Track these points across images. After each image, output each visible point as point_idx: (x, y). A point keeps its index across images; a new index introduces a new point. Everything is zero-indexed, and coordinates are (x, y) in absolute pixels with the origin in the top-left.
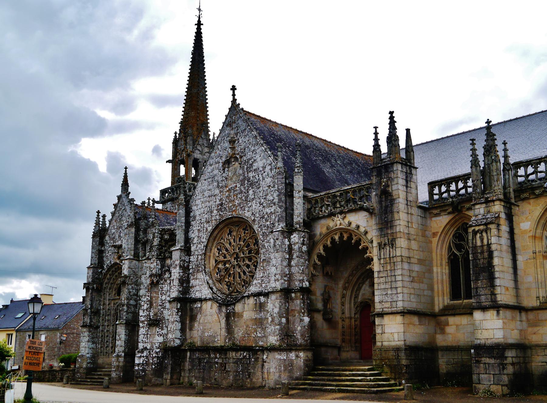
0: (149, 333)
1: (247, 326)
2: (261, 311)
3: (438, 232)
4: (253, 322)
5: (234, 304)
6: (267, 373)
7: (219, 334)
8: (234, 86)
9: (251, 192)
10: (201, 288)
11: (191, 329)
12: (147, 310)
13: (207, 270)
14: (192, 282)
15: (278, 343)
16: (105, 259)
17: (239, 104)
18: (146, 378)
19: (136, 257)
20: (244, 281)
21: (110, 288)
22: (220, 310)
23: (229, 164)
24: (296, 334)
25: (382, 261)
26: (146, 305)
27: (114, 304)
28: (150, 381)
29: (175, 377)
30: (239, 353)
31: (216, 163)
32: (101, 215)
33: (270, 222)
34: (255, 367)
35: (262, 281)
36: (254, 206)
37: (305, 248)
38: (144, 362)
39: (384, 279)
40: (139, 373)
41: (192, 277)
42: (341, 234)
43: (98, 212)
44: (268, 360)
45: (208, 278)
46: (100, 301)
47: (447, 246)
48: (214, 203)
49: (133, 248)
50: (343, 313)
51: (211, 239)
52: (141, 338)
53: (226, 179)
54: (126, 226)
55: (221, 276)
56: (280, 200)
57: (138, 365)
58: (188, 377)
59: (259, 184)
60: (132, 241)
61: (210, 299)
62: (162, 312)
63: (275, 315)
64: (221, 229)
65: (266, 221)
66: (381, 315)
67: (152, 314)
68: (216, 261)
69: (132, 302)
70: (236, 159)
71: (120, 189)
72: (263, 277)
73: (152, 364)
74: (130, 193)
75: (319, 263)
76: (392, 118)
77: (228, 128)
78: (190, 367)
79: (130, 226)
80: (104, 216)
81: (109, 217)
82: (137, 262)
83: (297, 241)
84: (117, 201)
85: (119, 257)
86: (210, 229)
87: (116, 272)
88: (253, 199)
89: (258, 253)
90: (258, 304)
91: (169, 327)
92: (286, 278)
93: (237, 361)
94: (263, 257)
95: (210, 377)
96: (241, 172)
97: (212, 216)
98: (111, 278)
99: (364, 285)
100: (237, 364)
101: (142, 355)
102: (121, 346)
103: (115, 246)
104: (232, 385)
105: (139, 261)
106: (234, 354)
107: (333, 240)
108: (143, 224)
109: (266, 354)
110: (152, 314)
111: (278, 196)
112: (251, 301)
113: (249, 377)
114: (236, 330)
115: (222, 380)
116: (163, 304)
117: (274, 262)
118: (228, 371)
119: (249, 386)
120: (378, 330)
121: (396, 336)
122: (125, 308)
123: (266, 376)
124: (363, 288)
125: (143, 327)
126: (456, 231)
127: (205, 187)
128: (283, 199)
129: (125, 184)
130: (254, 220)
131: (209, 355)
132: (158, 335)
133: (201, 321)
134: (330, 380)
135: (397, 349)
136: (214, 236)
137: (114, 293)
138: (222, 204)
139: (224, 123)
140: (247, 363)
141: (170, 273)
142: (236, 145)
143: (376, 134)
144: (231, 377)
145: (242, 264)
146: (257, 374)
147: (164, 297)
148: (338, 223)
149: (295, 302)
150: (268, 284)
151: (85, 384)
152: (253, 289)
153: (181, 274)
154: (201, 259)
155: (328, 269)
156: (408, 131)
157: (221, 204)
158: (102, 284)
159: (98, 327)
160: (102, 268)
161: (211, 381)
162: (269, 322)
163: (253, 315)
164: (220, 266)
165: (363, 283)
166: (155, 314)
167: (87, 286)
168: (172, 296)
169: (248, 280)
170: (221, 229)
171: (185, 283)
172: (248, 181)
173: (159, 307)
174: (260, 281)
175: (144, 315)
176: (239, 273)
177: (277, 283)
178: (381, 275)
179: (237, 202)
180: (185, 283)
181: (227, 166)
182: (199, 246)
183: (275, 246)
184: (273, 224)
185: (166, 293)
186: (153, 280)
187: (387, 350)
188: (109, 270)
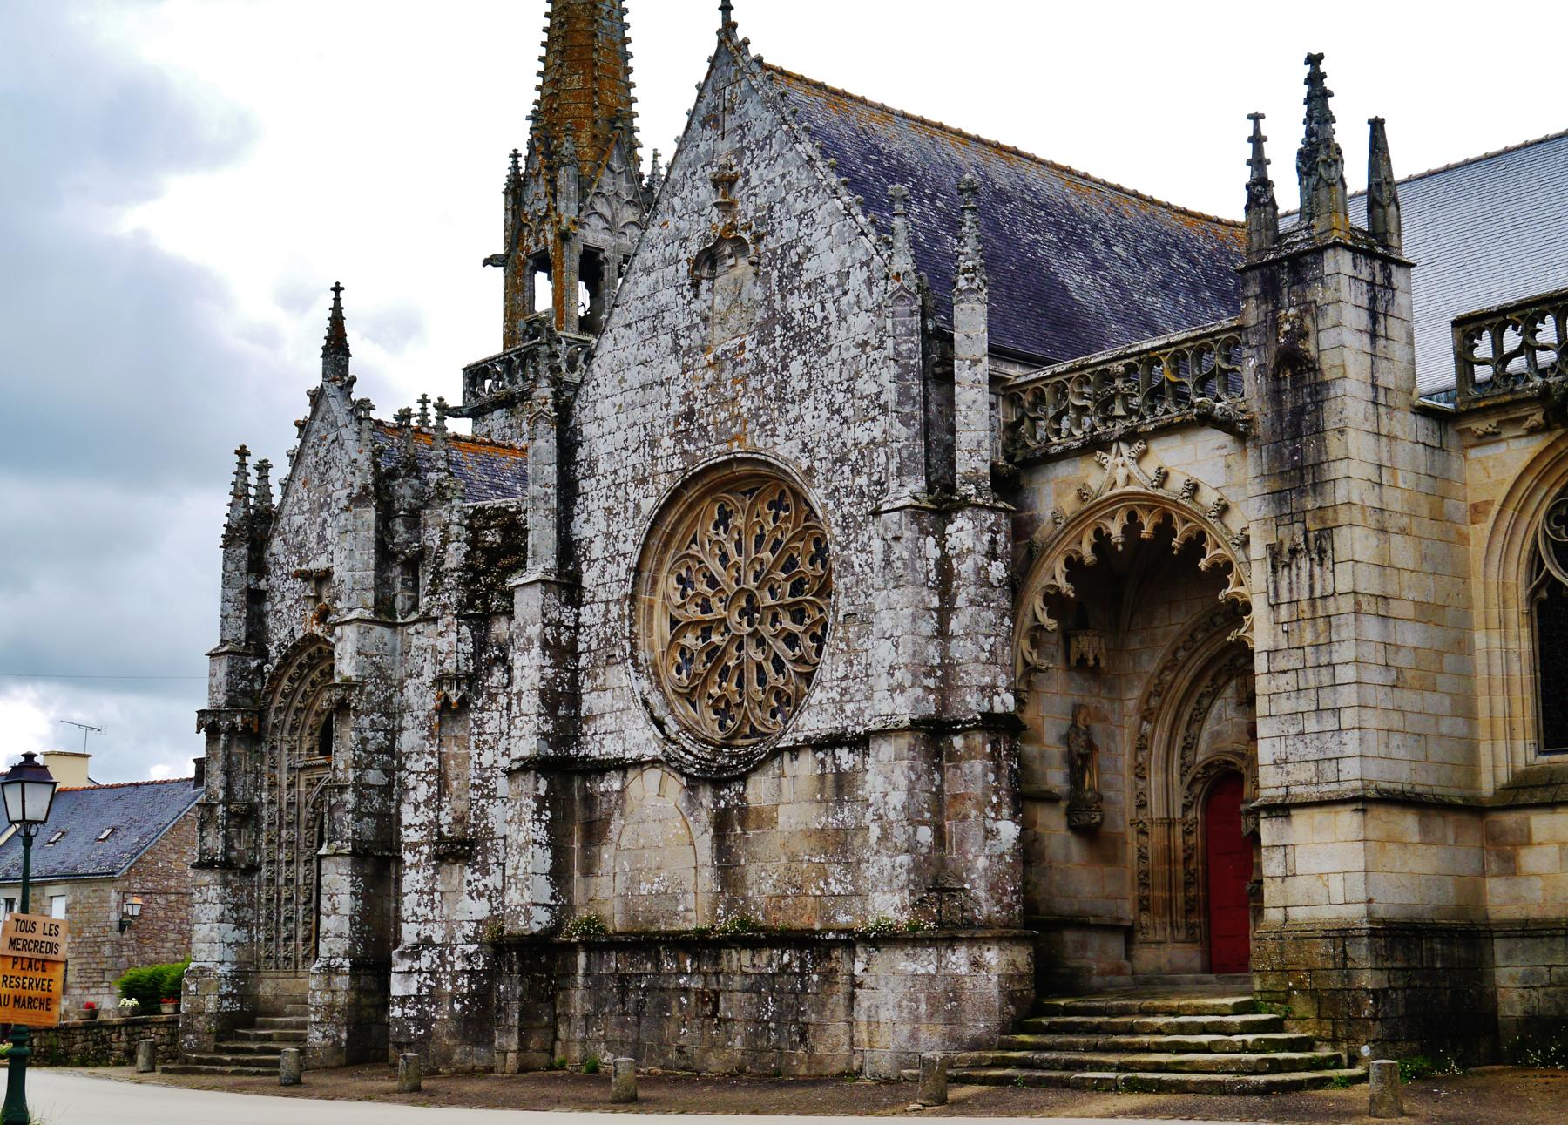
0: (439, 887)
1: (793, 858)
2: (840, 803)
3: (1489, 503)
4: (813, 842)
5: (743, 778)
6: (869, 1023)
7: (688, 886)
9: (796, 368)
10: (619, 721)
11: (588, 872)
12: (427, 802)
13: (641, 657)
14: (590, 701)
15: (904, 918)
16: (270, 622)
17: (746, 43)
18: (432, 1049)
19: (384, 613)
20: (779, 694)
21: (293, 729)
22: (692, 800)
23: (713, 267)
24: (972, 882)
25: (1284, 610)
27: (310, 784)
28: (446, 1059)
29: (534, 1043)
30: (766, 954)
31: (666, 263)
32: (252, 462)
33: (870, 475)
34: (824, 1005)
35: (844, 691)
36: (808, 418)
37: (998, 571)
38: (424, 991)
39: (1291, 677)
40: (404, 1031)
41: (587, 684)
42: (1132, 516)
43: (242, 452)
44: (869, 980)
45: (645, 684)
46: (259, 774)
47: (1525, 554)
48: (662, 411)
49: (371, 582)
50: (1142, 806)
51: (654, 541)
52: (409, 904)
53: (705, 319)
54: (344, 502)
55: (693, 676)
56: (904, 395)
57: (403, 1000)
58: (583, 1042)
59: (827, 337)
60: (367, 556)
61: (655, 762)
62: (483, 810)
63: (892, 816)
64: (691, 507)
65: (856, 471)
66: (1282, 809)
67: (445, 819)
68: (674, 622)
69: (374, 777)
70: (740, 246)
71: (317, 365)
72: (846, 677)
73: (453, 998)
74: (354, 379)
75: (1051, 624)
76: (1315, 80)
77: (708, 133)
78: (588, 1007)
79: (357, 500)
80: (263, 467)
81: (280, 470)
82: (387, 632)
83: (969, 543)
84: (308, 411)
85: (323, 616)
86: (648, 505)
87: (312, 668)
88: (805, 393)
89: (825, 589)
90: (830, 778)
91: (508, 863)
92: (931, 682)
93: (759, 985)
94: (844, 606)
95: (661, 1043)
96: (759, 293)
97: (654, 458)
98: (294, 692)
99: (1218, 703)
100: (759, 993)
101: (416, 966)
102: (340, 935)
103: (306, 576)
104: (742, 1070)
105: (393, 626)
106: (746, 956)
107: (1102, 538)
108: (405, 491)
109: (864, 957)
110: (445, 819)
111: (898, 378)
112: (807, 764)
113: (803, 1039)
114: (752, 872)
115: (706, 1051)
116: (487, 780)
117: (885, 622)
118: (726, 1020)
119: (802, 1071)
120: (1271, 865)
121: (1336, 884)
122: (349, 797)
123: (865, 1036)
124: (1214, 712)
125: (415, 865)
126: (1559, 495)
127: (629, 354)
128: (916, 389)
129: (336, 347)
130: (810, 471)
131: (658, 963)
132: (470, 893)
133: (624, 842)
134: (1096, 1049)
135: (1342, 934)
136: (664, 529)
137: (306, 745)
138: (691, 409)
139: (692, 114)
140: (793, 991)
141: (509, 670)
142: (738, 192)
143: (1257, 140)
144: (738, 1043)
145: (767, 631)
146: (832, 1030)
147: (487, 758)
148: (1120, 474)
149: (966, 766)
150: (863, 704)
151: (214, 1072)
152: (812, 722)
153: (549, 672)
154: (621, 618)
155: (1087, 645)
156: (1377, 125)
157: (689, 415)
158: (262, 714)
159: (253, 869)
160: (263, 654)
161: (664, 1055)
162: (873, 840)
164: (691, 640)
165: (1215, 694)
166: (460, 820)
167: (209, 723)
168: (516, 754)
169: (791, 689)
170: (691, 507)
171: (563, 703)
172: (785, 327)
173: (473, 794)
174: (835, 694)
175: (417, 821)
176: (760, 666)
177: (900, 699)
178: (1281, 663)
179: (745, 405)
180: (563, 703)
181: (705, 272)
182: (612, 568)
183: (888, 563)
184: (879, 483)
185: (497, 741)
186: (447, 697)
187: (1304, 937)
188: (286, 661)
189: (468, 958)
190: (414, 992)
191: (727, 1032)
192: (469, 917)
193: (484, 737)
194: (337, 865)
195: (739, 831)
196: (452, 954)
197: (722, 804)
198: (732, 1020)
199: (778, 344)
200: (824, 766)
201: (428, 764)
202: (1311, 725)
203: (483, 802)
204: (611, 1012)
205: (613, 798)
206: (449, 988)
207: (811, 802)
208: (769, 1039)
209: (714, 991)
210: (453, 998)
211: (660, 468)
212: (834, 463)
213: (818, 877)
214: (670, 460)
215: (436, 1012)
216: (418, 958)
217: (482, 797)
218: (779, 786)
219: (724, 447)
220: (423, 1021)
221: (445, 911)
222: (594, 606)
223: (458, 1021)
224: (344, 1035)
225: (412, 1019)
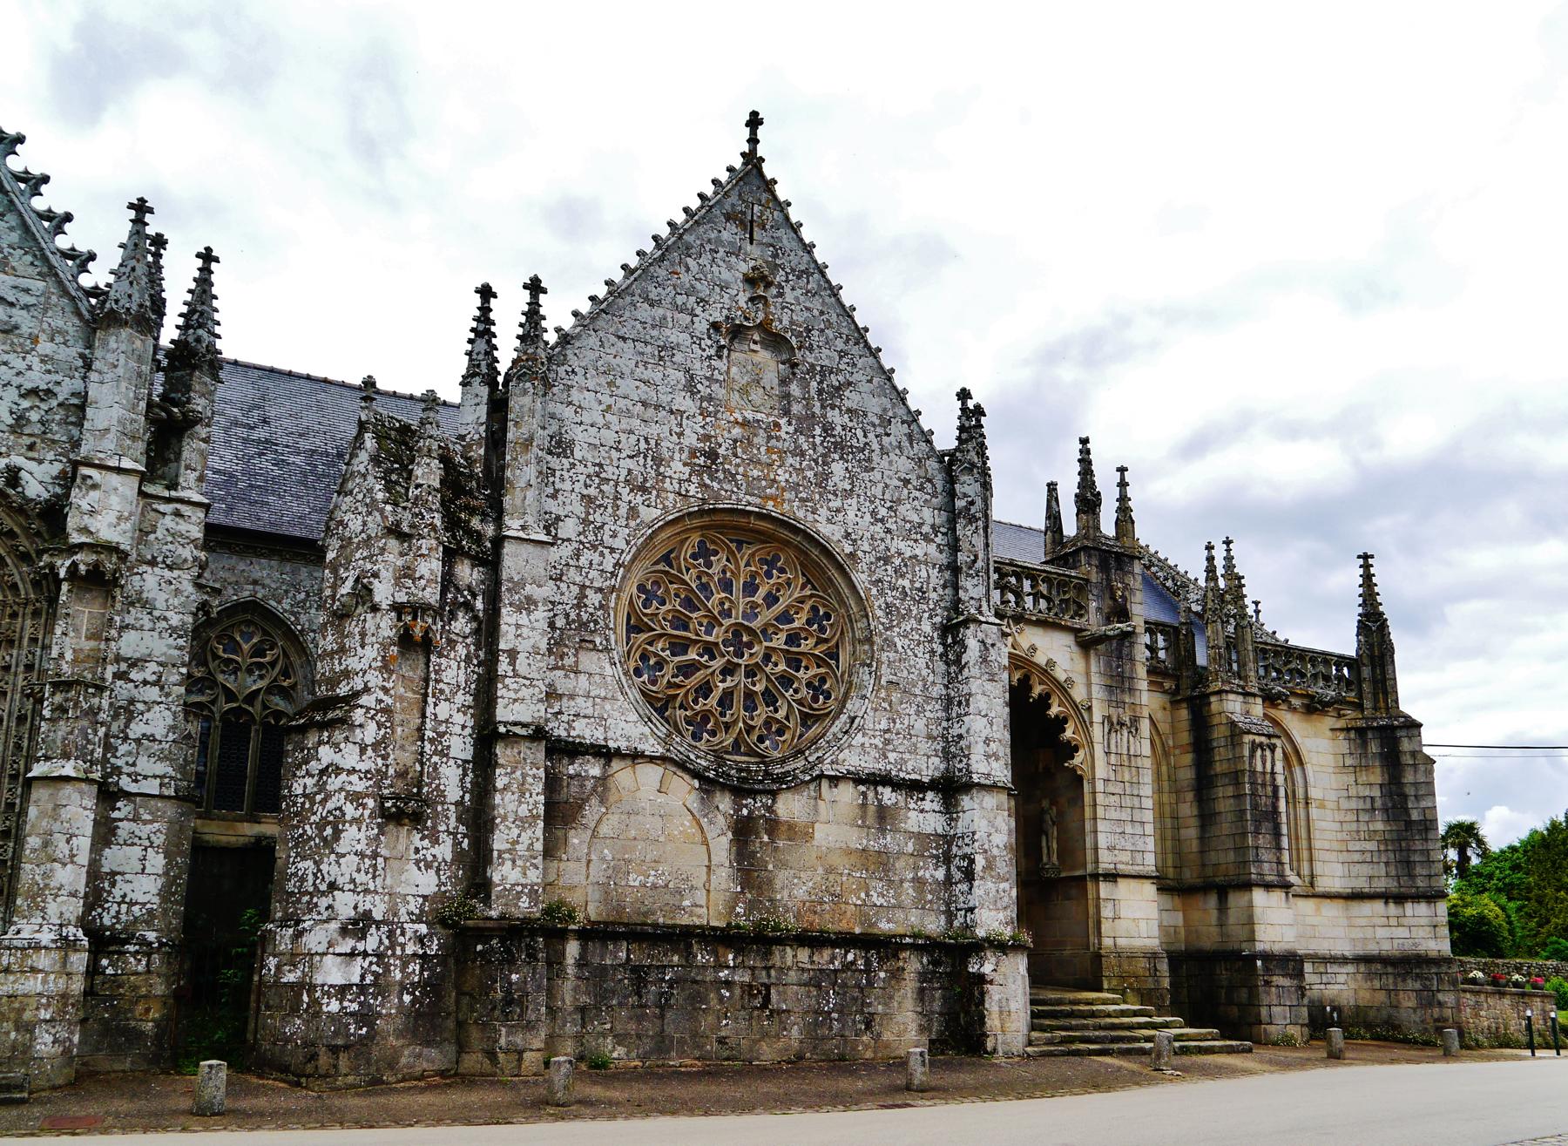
0: (383, 851)
1: (830, 870)
2: (882, 831)
4: (853, 859)
5: (774, 794)
6: (1001, 1012)
7: (699, 882)
8: (754, 114)
9: (838, 468)
15: (1008, 932)
18: (375, 1053)
25: (1113, 759)
26: (372, 726)
28: (392, 1065)
30: (827, 953)
33: (912, 582)
34: (891, 998)
35: (887, 742)
36: (851, 514)
38: (369, 979)
39: (1116, 798)
40: (342, 1030)
44: (998, 978)
57: (342, 991)
58: (579, 1038)
59: (869, 460)
61: (652, 759)
62: (436, 769)
63: (995, 851)
66: (1113, 877)
70: (775, 341)
72: (888, 731)
73: (403, 988)
76: (1085, 452)
78: (585, 999)
86: (649, 514)
90: (872, 809)
93: (817, 980)
95: (695, 1034)
100: (819, 987)
101: (360, 946)
102: (73, 895)
104: (800, 1057)
106: (803, 955)
109: (993, 960)
112: (847, 794)
113: (868, 1026)
115: (756, 1042)
117: (979, 702)
118: (780, 1012)
119: (869, 1055)
120: (1106, 912)
121: (1143, 925)
123: (997, 1023)
125: (357, 821)
130: (852, 555)
131: (688, 955)
132: (417, 862)
133: (604, 830)
135: (1153, 956)
140: (858, 986)
144: (795, 1031)
146: (899, 1018)
150: (907, 756)
152: (852, 760)
161: (700, 1047)
163: (856, 839)
172: (825, 430)
174: (878, 741)
175: (363, 767)
178: (1111, 789)
184: (920, 590)
187: (1132, 956)
189: (420, 940)
190: (356, 980)
191: (781, 1022)
193: (441, 686)
194: (81, 793)
195: (766, 838)
196: (403, 934)
197: (745, 812)
198: (788, 1011)
199: (818, 440)
200: (865, 797)
201: (380, 701)
202: (1129, 829)
203: (435, 759)
204: (620, 1004)
205: (589, 784)
206: (398, 976)
207: (852, 825)
208: (831, 1028)
209: (763, 984)
210: (403, 988)
211: (667, 485)
212: (879, 559)
213: (859, 889)
214: (679, 486)
215: (382, 1005)
216: (364, 938)
217: (435, 753)
218: (816, 806)
219: (758, 501)
220: (365, 1017)
221: (388, 881)
222: (563, 586)
223: (408, 1017)
224: (76, 1039)
225: (352, 1014)
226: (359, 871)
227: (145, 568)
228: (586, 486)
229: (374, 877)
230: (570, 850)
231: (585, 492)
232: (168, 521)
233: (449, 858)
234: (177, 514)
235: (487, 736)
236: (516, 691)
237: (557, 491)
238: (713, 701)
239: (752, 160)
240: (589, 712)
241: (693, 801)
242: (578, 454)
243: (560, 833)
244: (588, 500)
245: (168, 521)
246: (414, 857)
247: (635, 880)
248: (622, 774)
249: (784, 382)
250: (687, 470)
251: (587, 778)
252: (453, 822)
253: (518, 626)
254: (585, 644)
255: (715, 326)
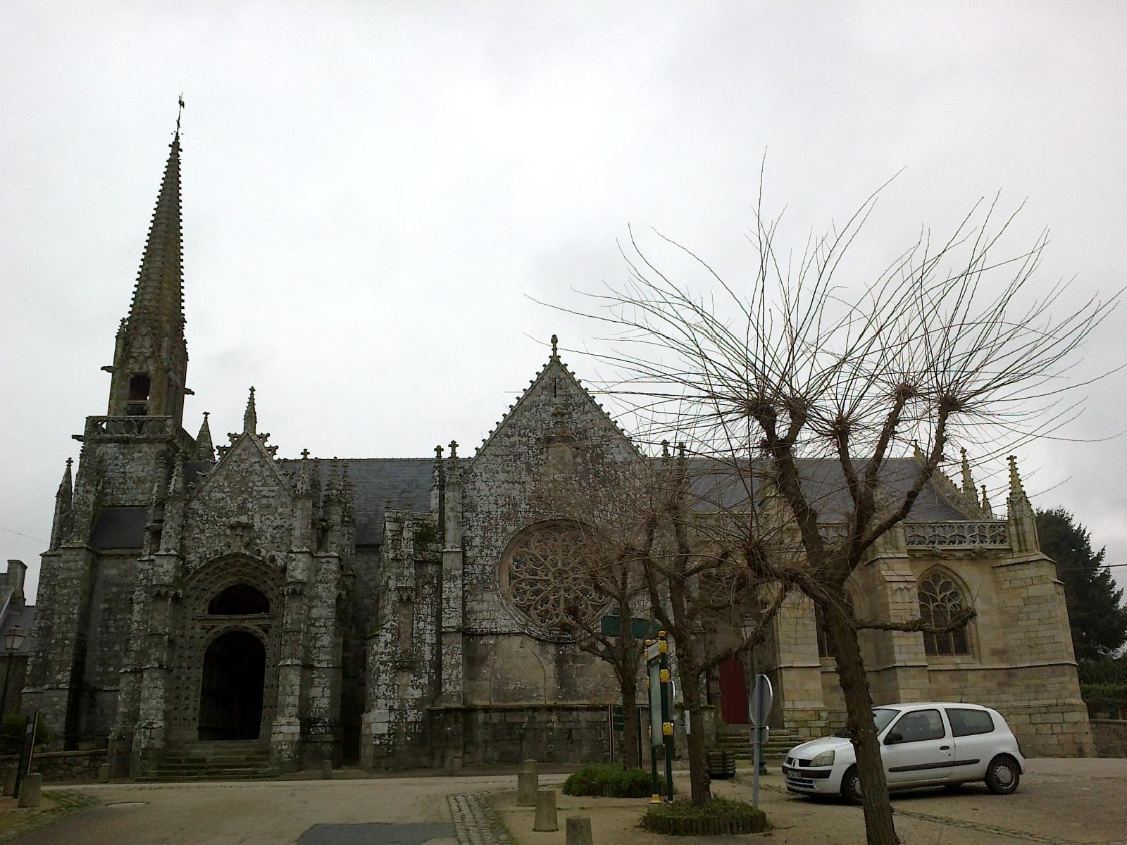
1: (604, 675)
61: (517, 634)
70: (567, 439)
86: (511, 529)
102: (294, 706)
132: (412, 687)
147: (421, 625)
166: (405, 652)
172: (595, 475)
175: (387, 651)
185: (426, 618)
192: (411, 697)
210: (407, 734)
217: (419, 642)
221: (400, 694)
226: (387, 691)
227: (319, 584)
228: (483, 522)
229: (394, 693)
230: (482, 675)
231: (483, 525)
232: (325, 566)
233: (427, 683)
234: (328, 562)
235: (440, 633)
236: (449, 614)
237: (471, 527)
238: (549, 606)
239: (555, 359)
240: (489, 617)
241: (537, 651)
242: (479, 510)
243: (477, 668)
244: (485, 529)
245: (325, 566)
246: (410, 684)
247: (511, 687)
248: (505, 642)
249: (574, 457)
250: (528, 507)
251: (488, 644)
252: (428, 669)
253: (450, 588)
254: (486, 589)
255: (538, 439)
